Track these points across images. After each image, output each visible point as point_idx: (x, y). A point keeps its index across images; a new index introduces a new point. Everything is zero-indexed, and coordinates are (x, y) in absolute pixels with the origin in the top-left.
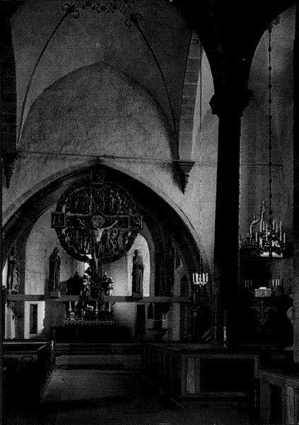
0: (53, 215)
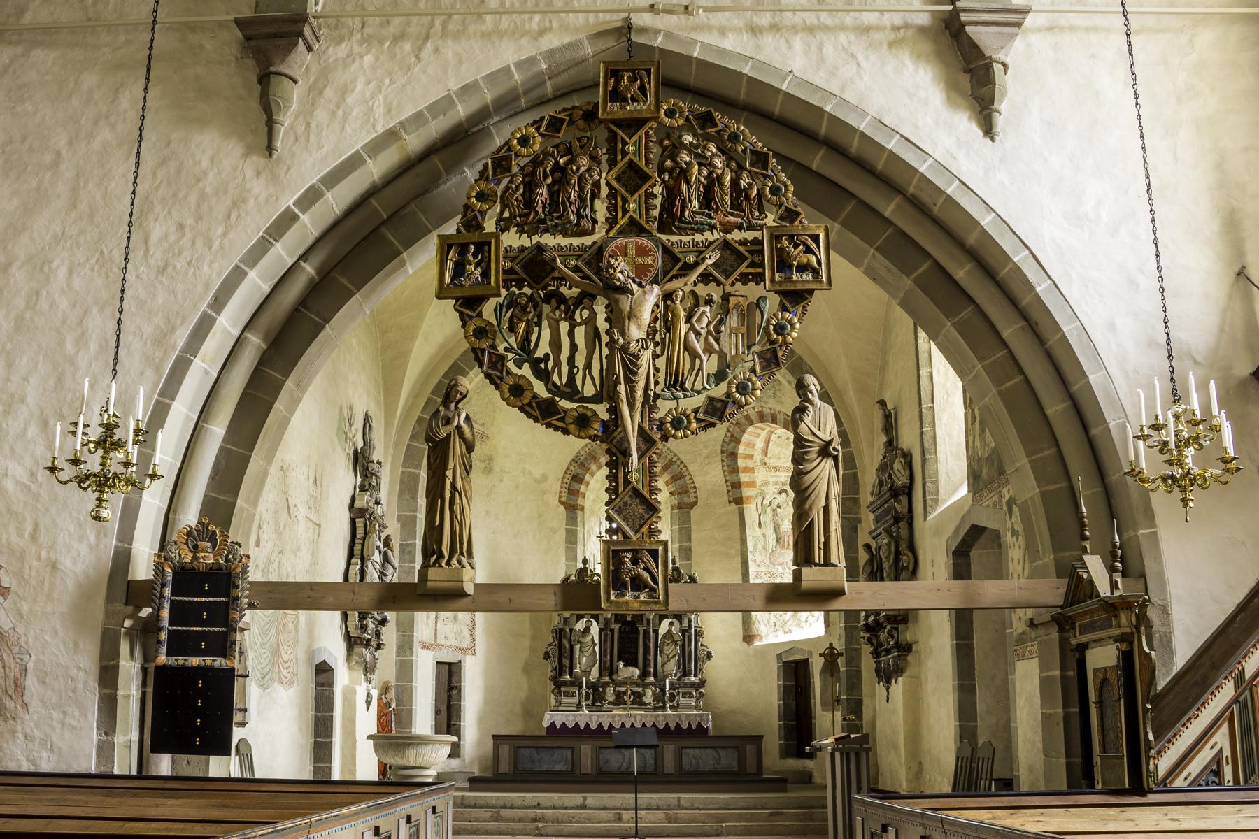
0: (446, 245)
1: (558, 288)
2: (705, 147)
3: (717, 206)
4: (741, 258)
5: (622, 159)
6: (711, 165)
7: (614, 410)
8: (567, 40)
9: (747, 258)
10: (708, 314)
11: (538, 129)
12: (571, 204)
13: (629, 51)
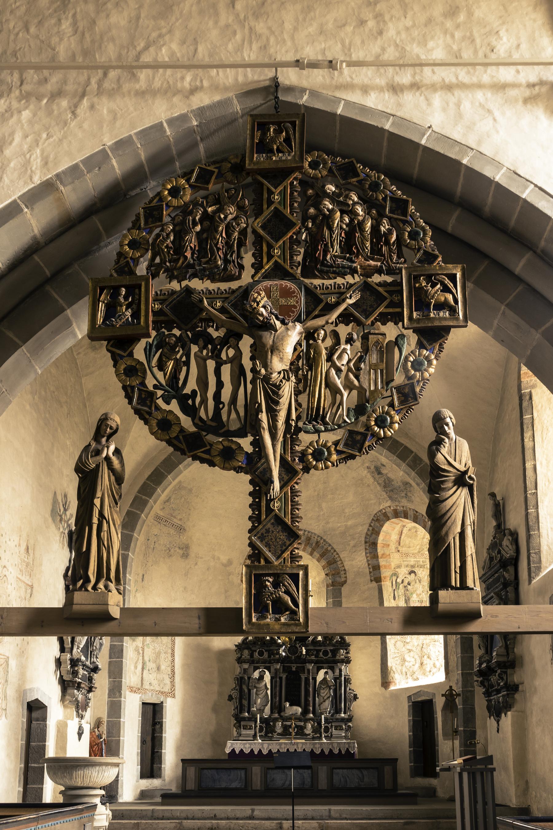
1: (205, 329)
2: (347, 197)
3: (358, 250)
4: (380, 298)
5: (268, 208)
6: (352, 213)
7: (258, 444)
8: (217, 98)
9: (386, 298)
10: (349, 352)
11: (188, 181)
12: (218, 249)
13: (275, 108)
